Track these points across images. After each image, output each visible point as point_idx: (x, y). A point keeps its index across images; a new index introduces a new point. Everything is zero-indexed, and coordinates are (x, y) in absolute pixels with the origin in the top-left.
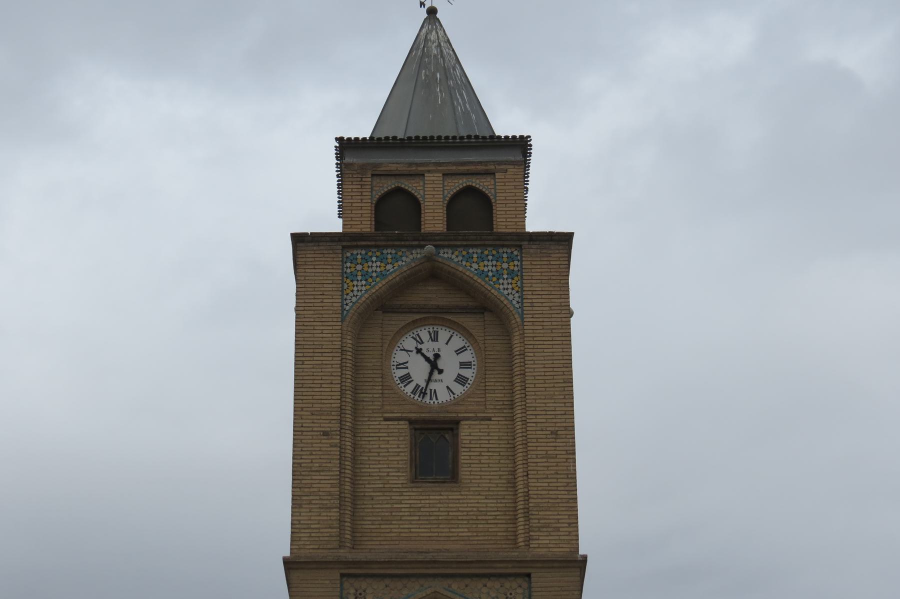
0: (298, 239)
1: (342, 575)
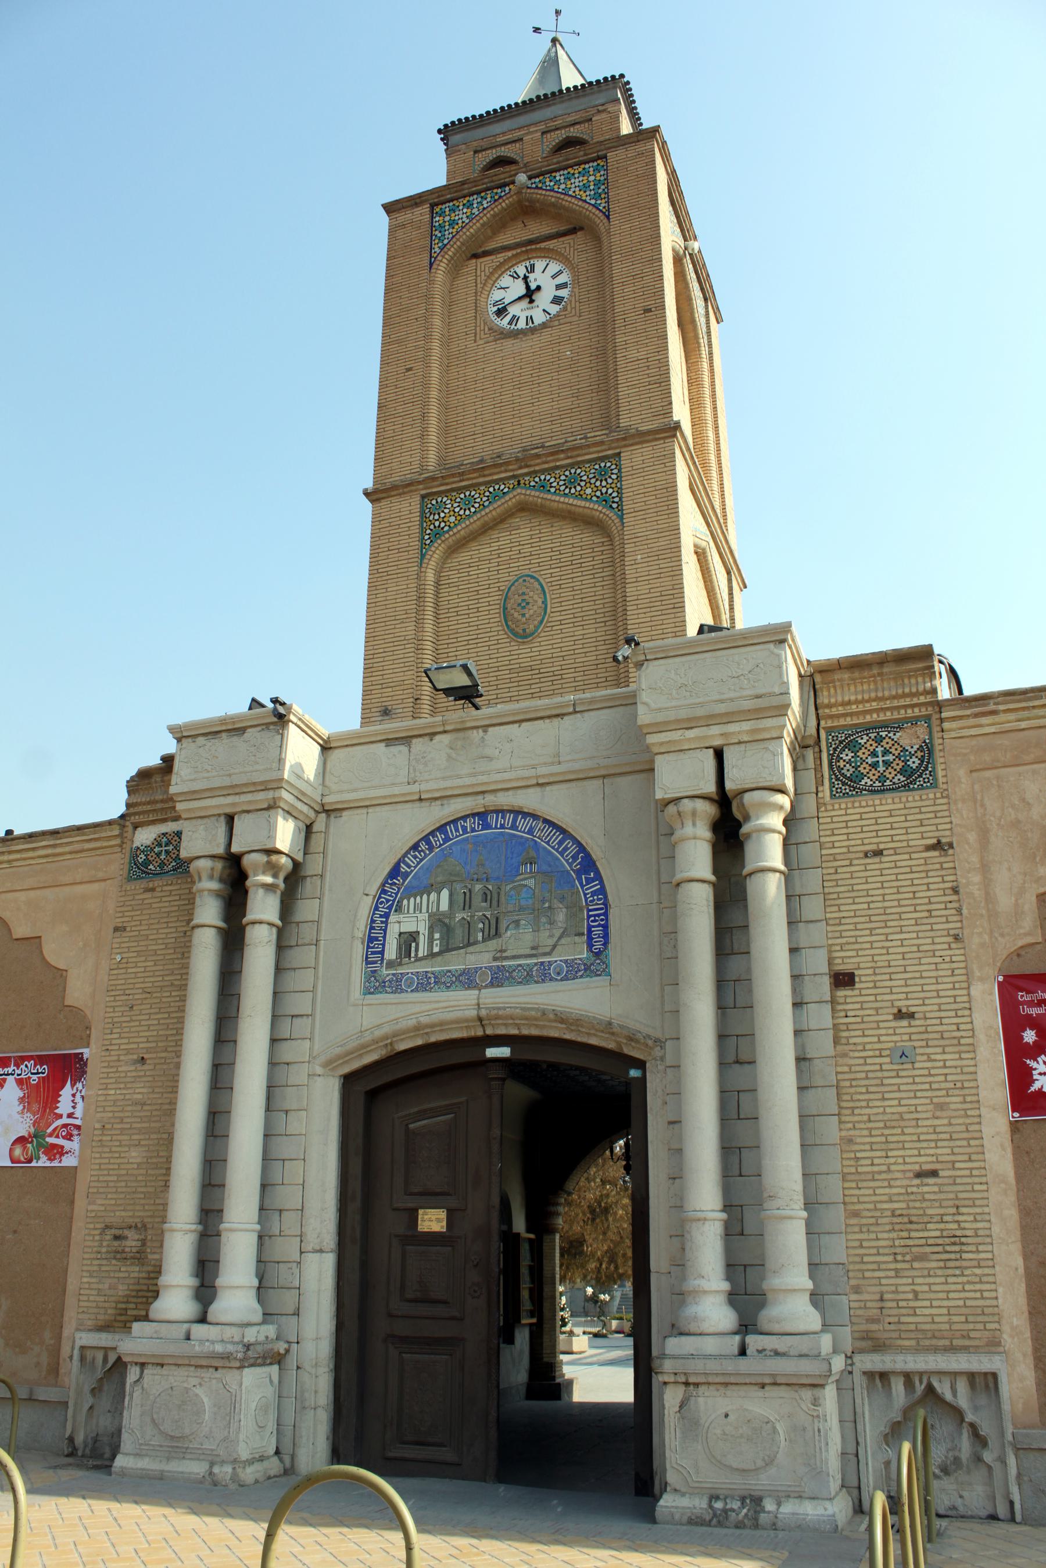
0: (390, 208)
1: (423, 497)
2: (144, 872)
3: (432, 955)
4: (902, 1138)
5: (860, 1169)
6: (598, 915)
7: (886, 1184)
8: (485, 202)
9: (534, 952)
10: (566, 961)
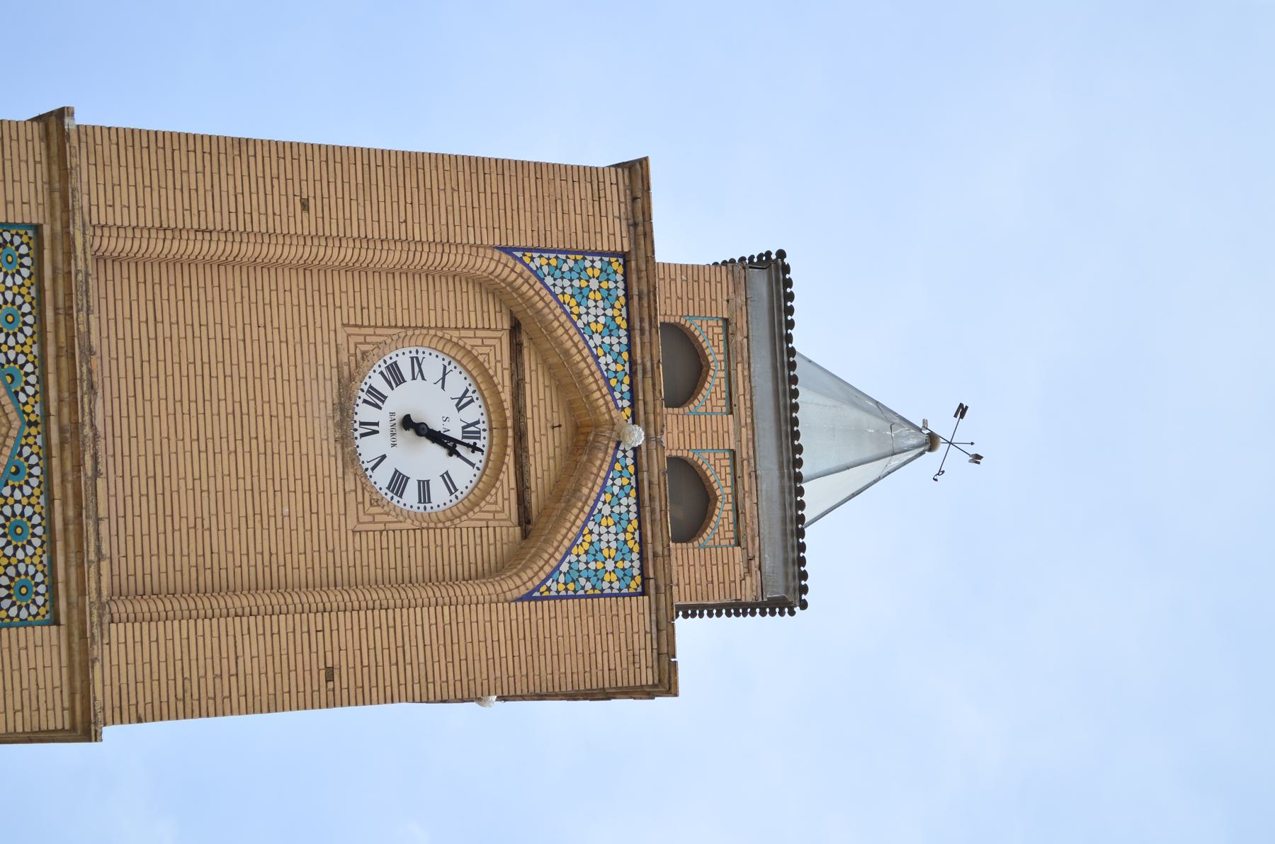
1: (37, 228)
8: (609, 359)
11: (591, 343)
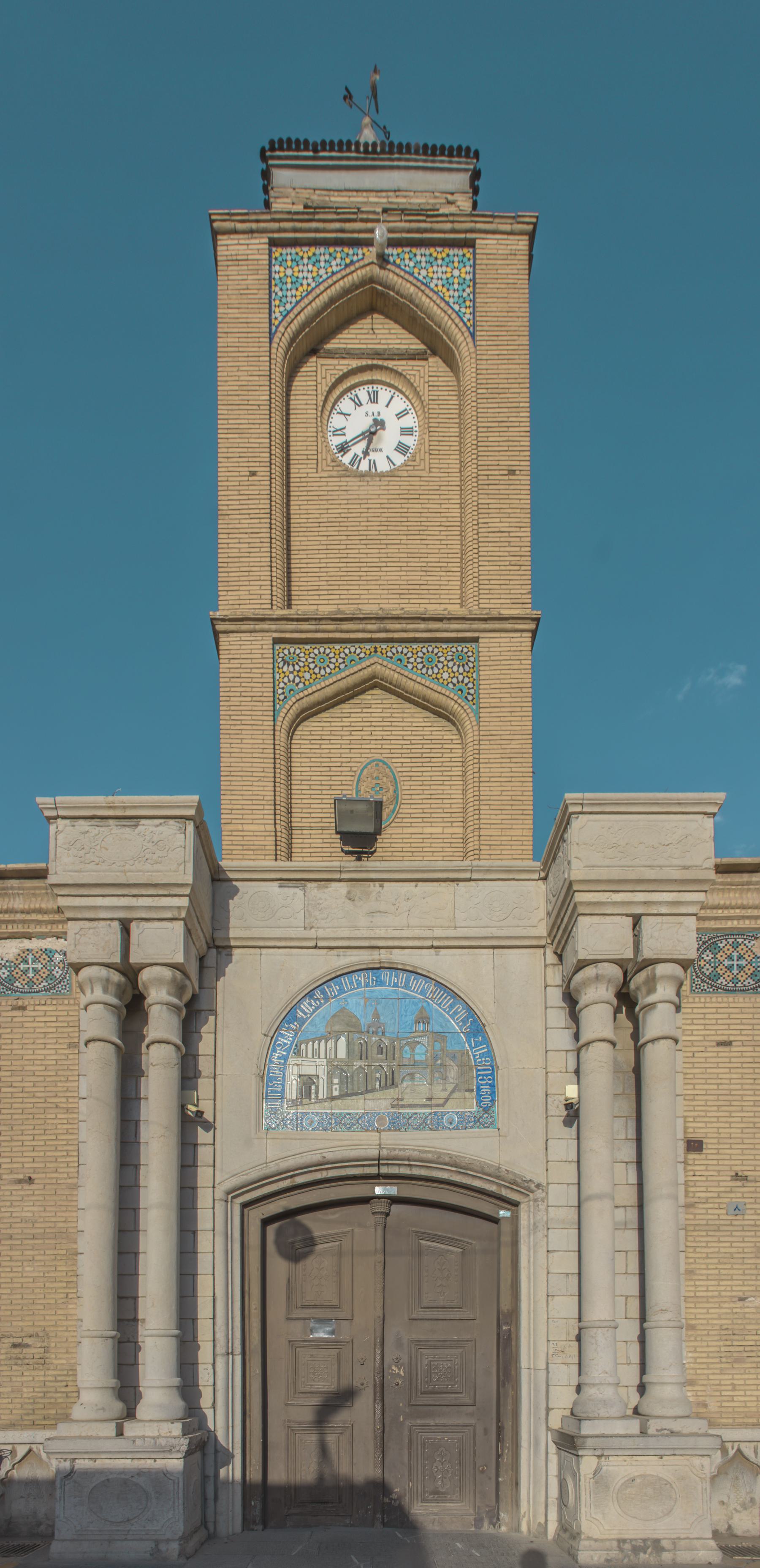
2: (8, 989)
3: (333, 1098)
4: (731, 1272)
5: (698, 1294)
6: (487, 1075)
7: (717, 1305)
9: (429, 1103)
10: (457, 1113)
11: (325, 277)
